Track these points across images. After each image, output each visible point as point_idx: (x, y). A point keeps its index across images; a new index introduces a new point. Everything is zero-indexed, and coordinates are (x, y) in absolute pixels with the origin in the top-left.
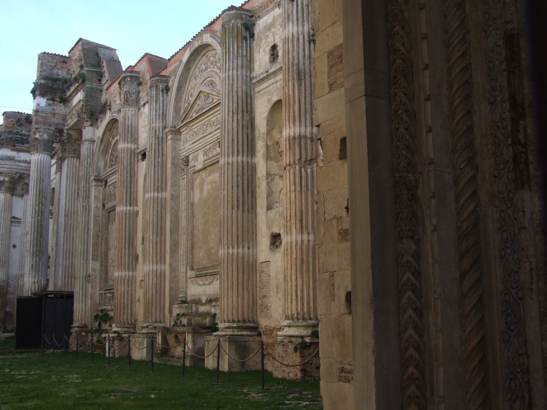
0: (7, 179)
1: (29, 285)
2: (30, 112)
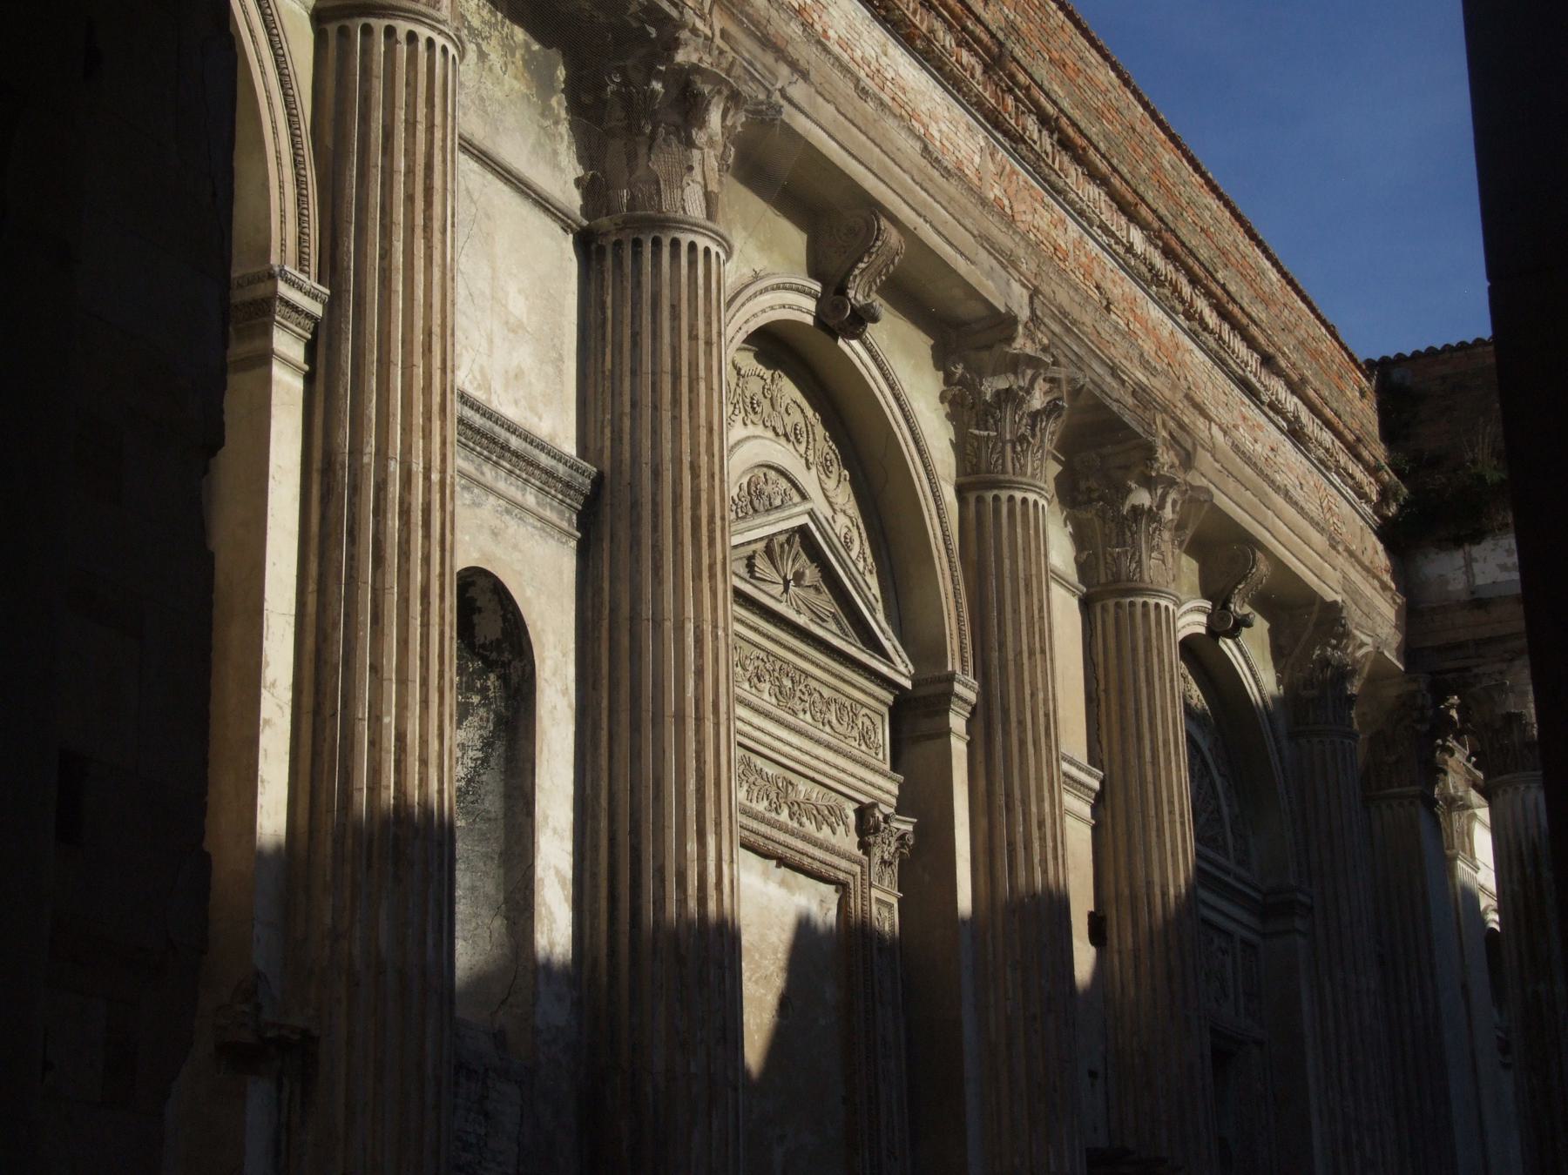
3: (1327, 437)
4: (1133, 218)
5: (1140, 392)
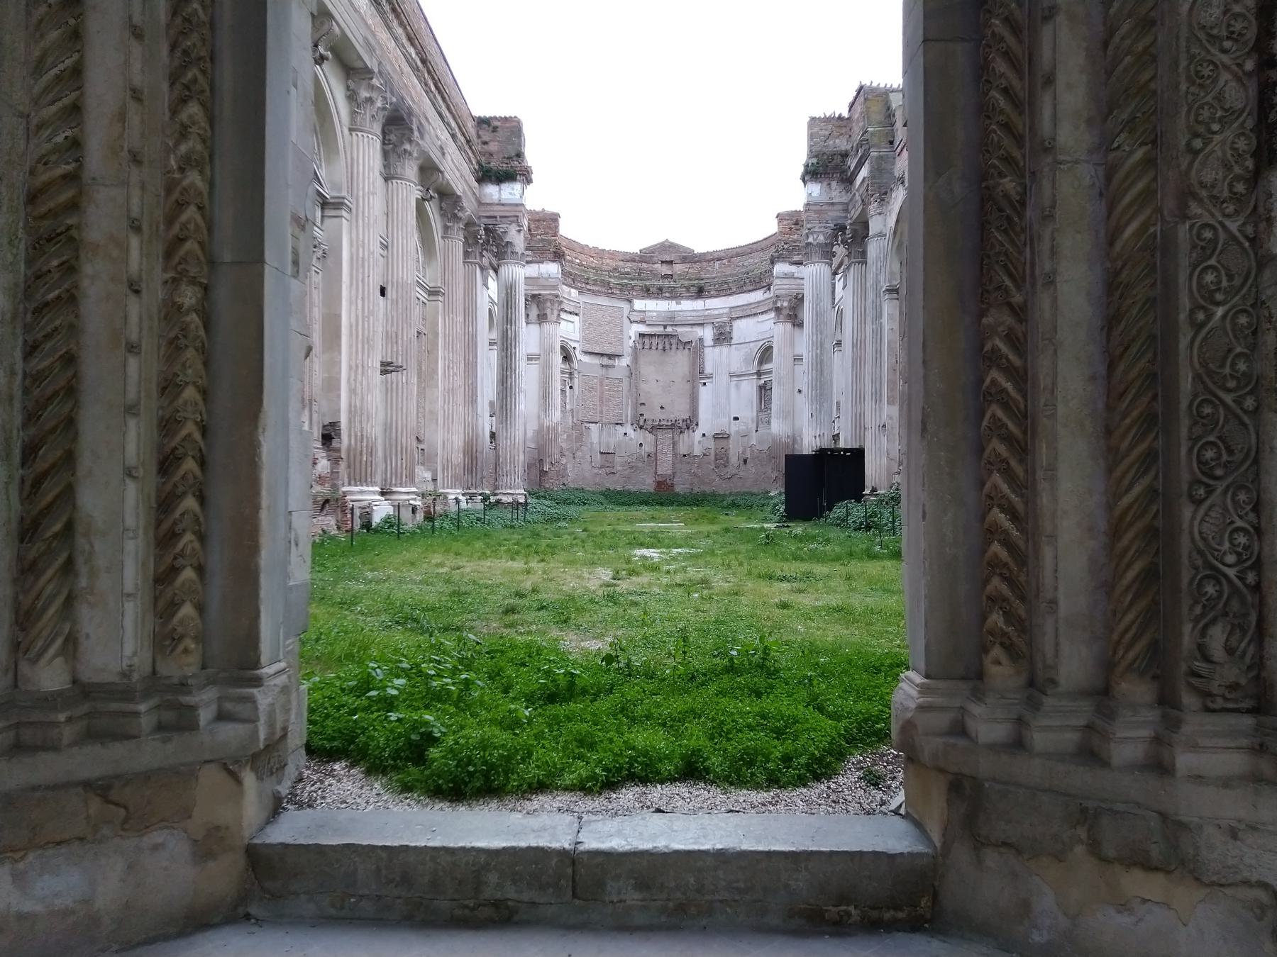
0: (786, 304)
1: (809, 443)
2: (800, 207)
3: (462, 139)
4: (413, 44)
5: (409, 108)
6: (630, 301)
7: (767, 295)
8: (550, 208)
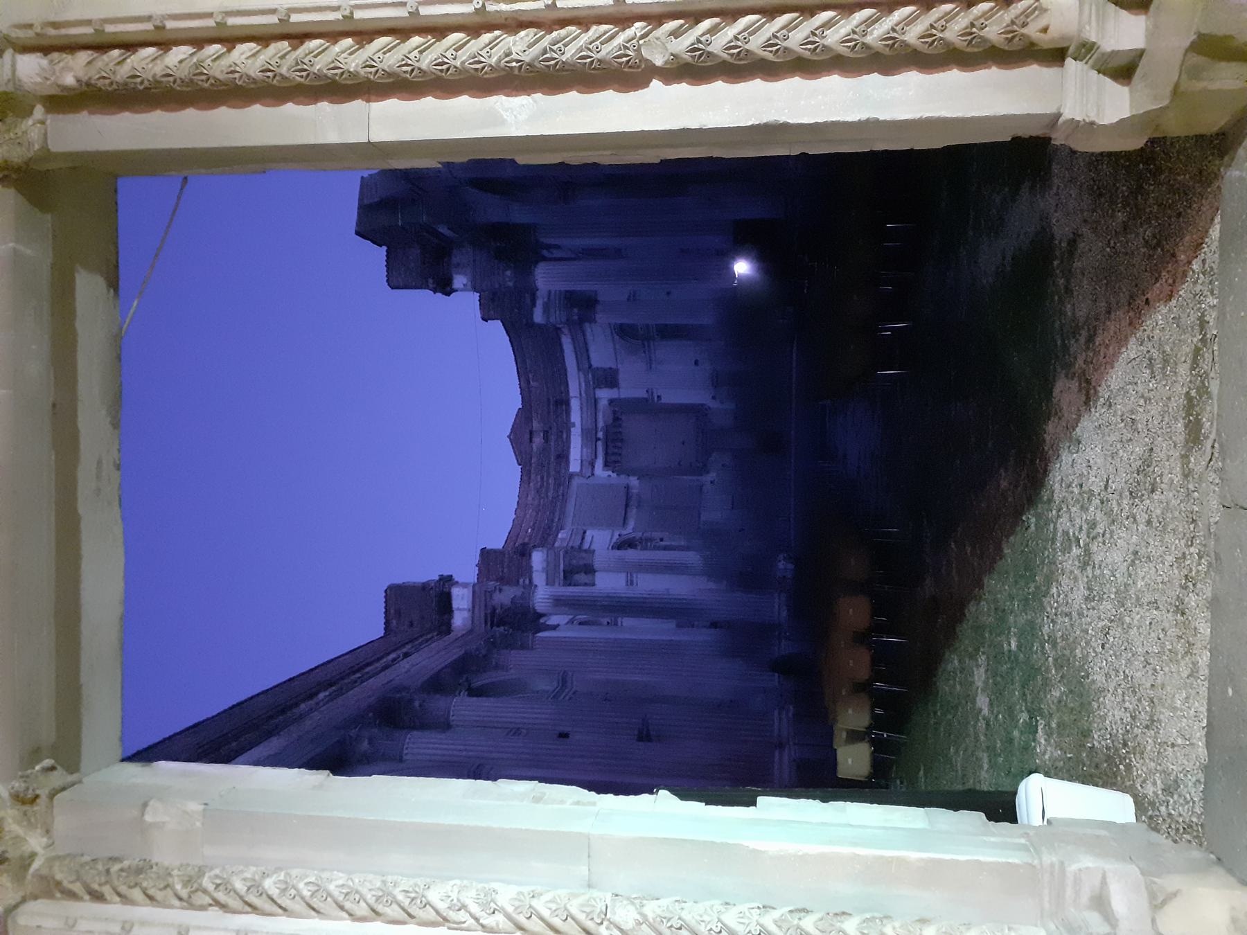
3: (409, 646)
4: (316, 694)
6: (571, 476)
7: (566, 331)
8: (476, 558)
